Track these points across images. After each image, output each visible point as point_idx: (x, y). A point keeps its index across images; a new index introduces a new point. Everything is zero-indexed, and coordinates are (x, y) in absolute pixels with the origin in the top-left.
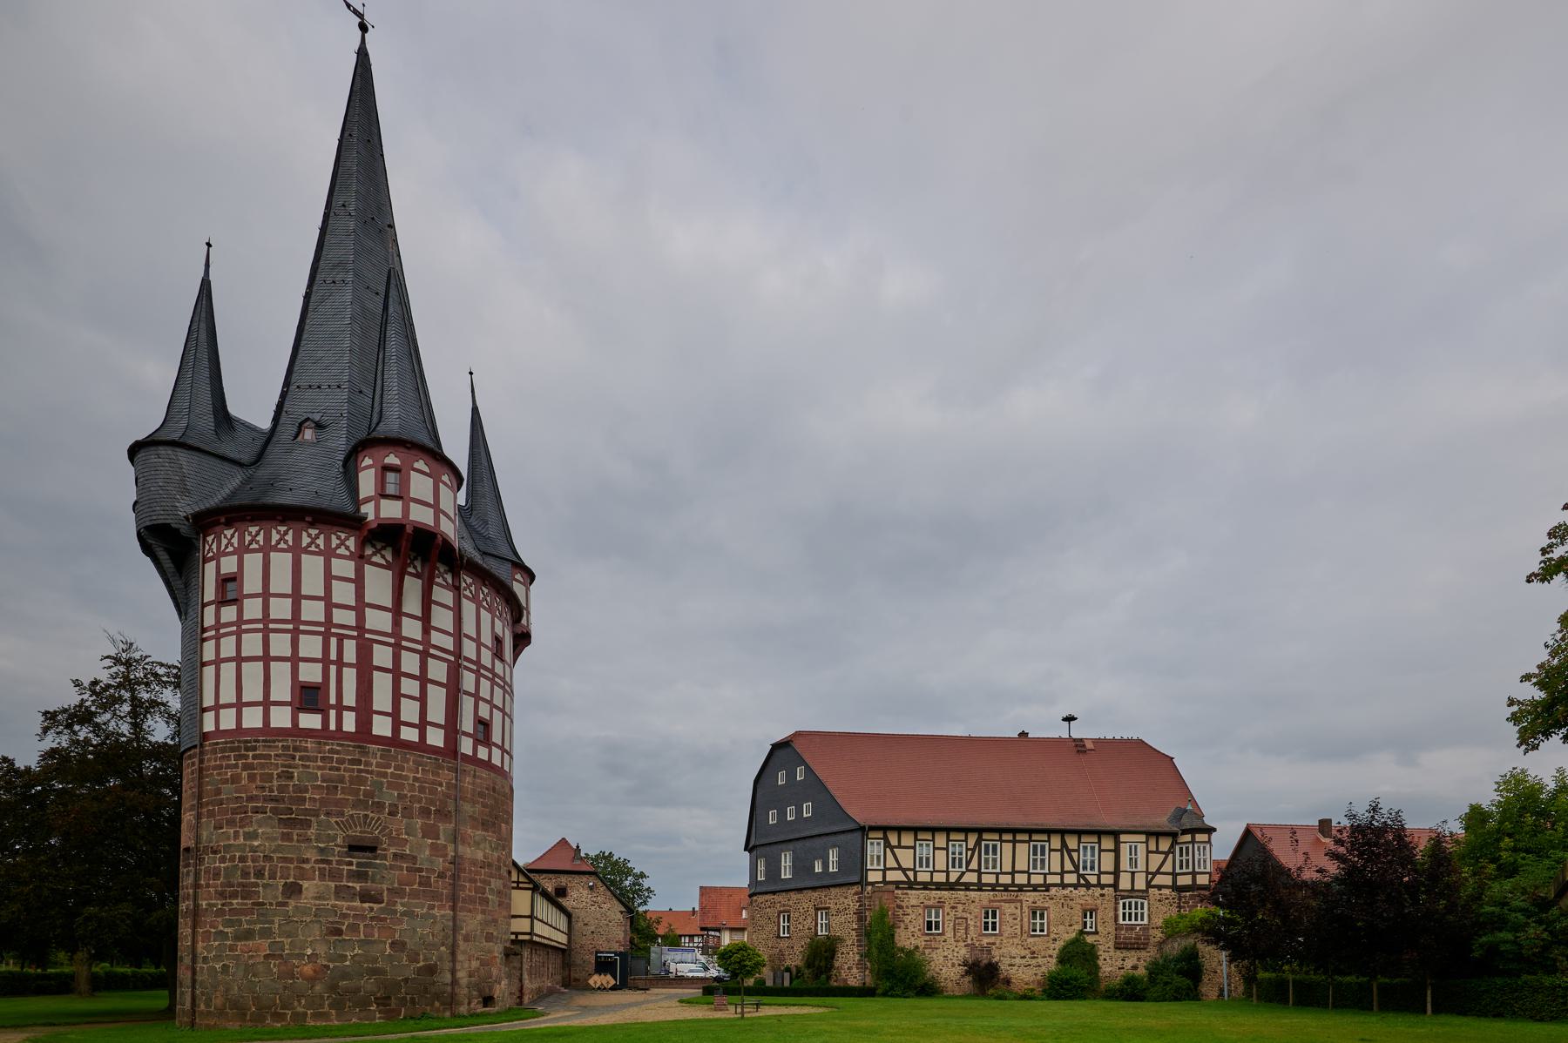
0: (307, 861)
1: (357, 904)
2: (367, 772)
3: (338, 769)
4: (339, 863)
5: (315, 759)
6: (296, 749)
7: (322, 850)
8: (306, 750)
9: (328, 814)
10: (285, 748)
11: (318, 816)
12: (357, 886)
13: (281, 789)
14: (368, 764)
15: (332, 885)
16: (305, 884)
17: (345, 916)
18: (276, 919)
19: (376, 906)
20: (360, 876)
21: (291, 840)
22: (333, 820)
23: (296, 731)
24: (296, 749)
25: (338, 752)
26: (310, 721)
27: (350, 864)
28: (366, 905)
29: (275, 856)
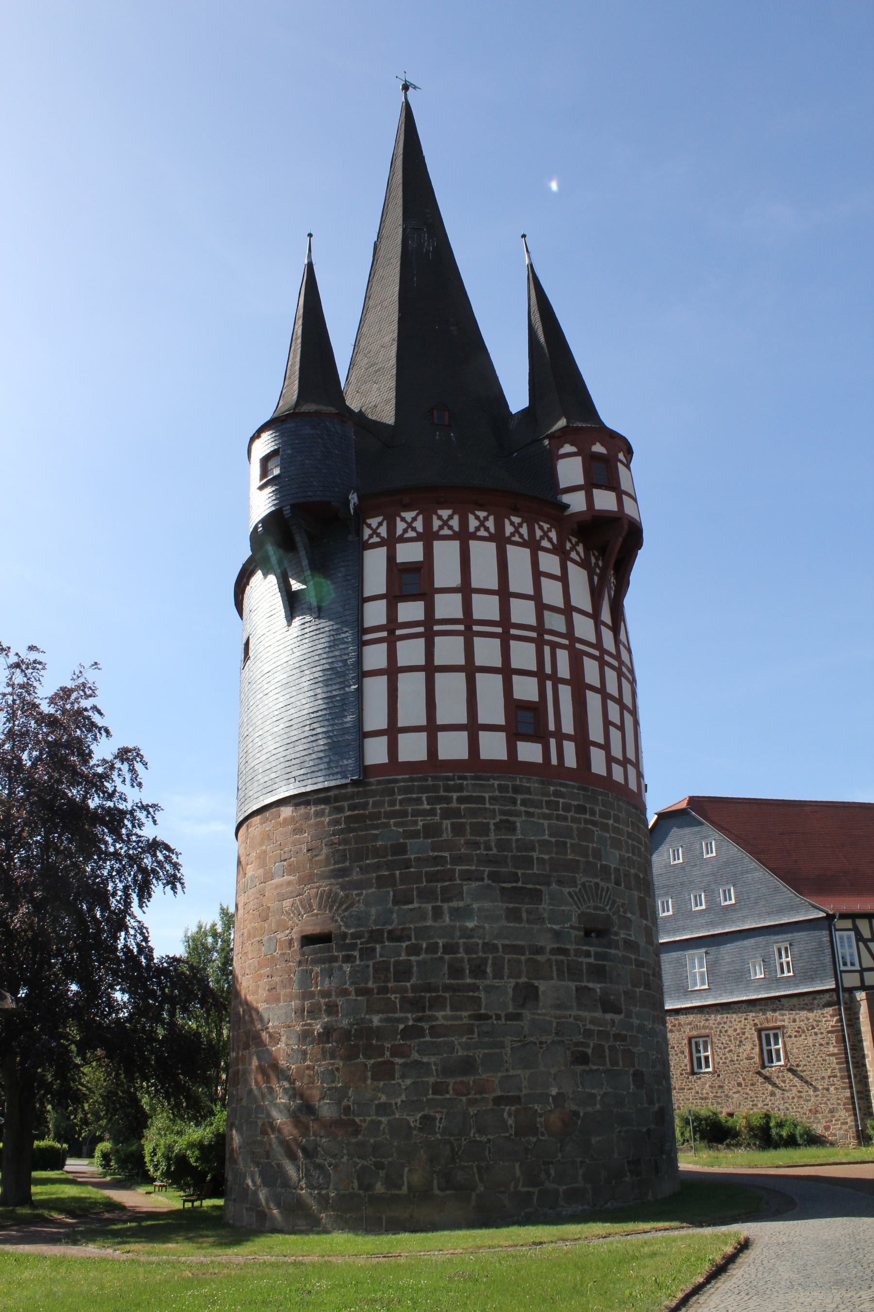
0: (540, 950)
1: (598, 1014)
2: (594, 823)
3: (565, 819)
4: (578, 953)
5: (538, 805)
6: (517, 790)
7: (557, 935)
8: (528, 791)
9: (560, 882)
10: (502, 788)
11: (548, 884)
12: (597, 987)
13: (503, 845)
14: (593, 813)
15: (573, 985)
16: (542, 986)
17: (588, 1033)
18: (507, 1040)
19: (617, 1018)
20: (598, 973)
21: (519, 919)
22: (566, 890)
23: (512, 764)
24: (517, 790)
25: (563, 796)
26: (529, 752)
27: (588, 954)
28: (609, 1016)
29: (499, 943)
